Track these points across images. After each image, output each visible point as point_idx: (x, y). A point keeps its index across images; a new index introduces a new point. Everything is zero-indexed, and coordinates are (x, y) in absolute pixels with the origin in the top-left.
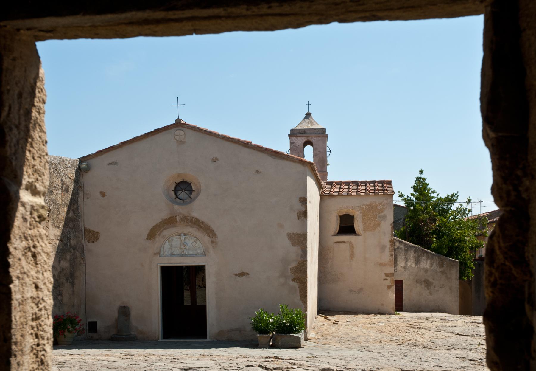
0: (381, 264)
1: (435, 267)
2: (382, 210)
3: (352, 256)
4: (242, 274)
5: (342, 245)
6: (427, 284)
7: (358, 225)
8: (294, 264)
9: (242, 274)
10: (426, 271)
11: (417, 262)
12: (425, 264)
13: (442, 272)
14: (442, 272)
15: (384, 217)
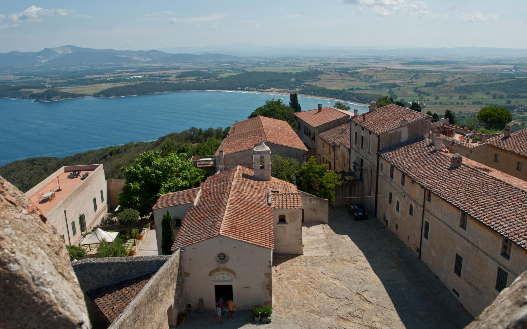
0: (297, 235)
1: (318, 203)
2: (297, 214)
3: (285, 232)
4: (247, 287)
5: (281, 228)
6: (315, 210)
7: (287, 220)
8: (267, 284)
9: (247, 287)
10: (314, 205)
11: (310, 201)
12: (314, 202)
13: (321, 205)
14: (321, 205)
15: (298, 217)
